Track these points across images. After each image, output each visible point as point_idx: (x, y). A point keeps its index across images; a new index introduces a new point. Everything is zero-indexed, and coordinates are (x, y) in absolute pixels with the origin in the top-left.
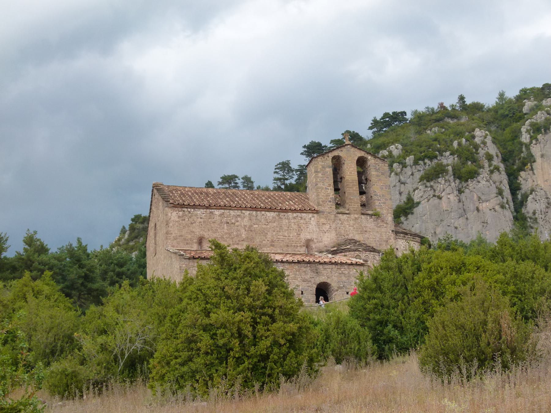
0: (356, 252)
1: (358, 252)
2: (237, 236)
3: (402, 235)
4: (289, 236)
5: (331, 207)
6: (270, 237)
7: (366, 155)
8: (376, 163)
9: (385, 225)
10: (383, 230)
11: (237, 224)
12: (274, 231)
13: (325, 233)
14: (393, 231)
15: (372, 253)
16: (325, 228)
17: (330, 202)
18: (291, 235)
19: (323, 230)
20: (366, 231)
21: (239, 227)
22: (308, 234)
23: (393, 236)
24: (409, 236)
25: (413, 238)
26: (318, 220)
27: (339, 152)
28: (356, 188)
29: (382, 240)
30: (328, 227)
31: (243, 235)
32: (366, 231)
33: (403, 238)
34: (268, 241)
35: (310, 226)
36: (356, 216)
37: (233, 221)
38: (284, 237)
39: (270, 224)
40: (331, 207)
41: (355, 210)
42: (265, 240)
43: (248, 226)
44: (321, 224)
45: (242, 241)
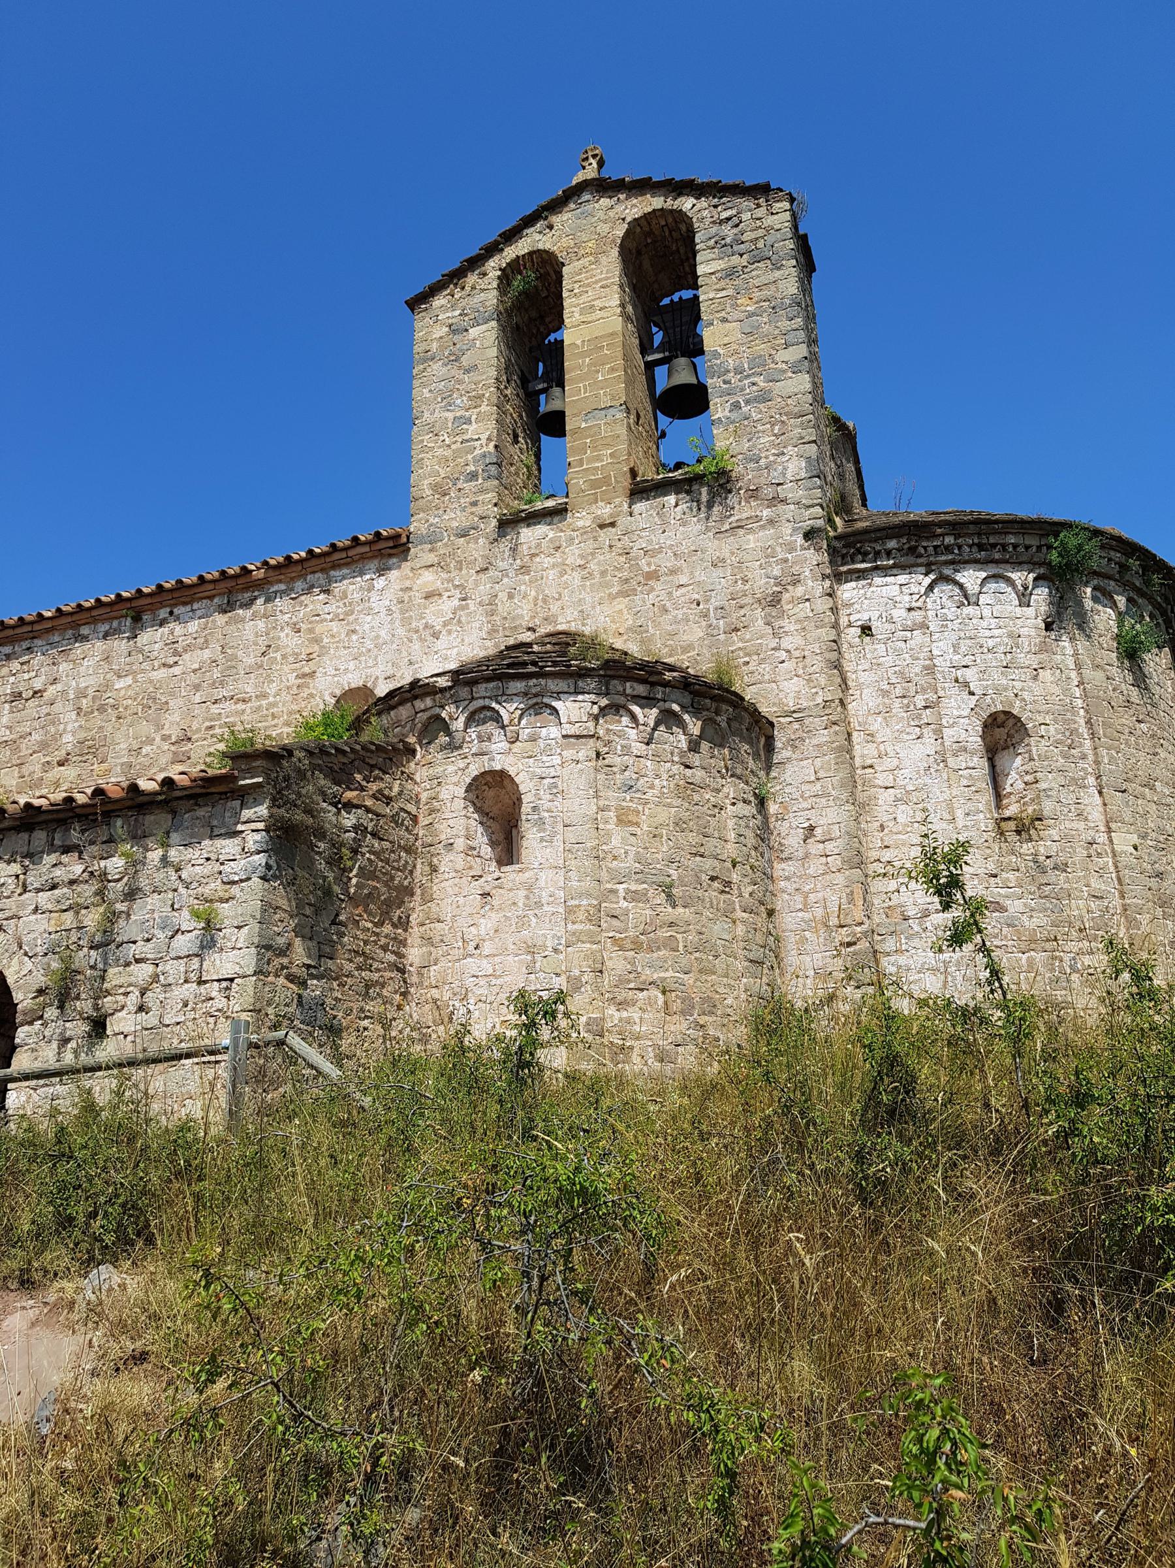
0: (419, 704)
1: (428, 702)
2: (43, 746)
3: (892, 544)
4: (264, 696)
5: (474, 504)
6: (176, 717)
7: (671, 204)
8: (725, 215)
9: (766, 513)
10: (752, 541)
11: (51, 691)
12: (197, 687)
13: (436, 635)
14: (809, 535)
15: (518, 686)
16: (440, 613)
17: (473, 476)
18: (272, 689)
19: (426, 626)
20: (653, 576)
21: (58, 707)
22: (352, 665)
23: (812, 559)
24: (949, 540)
25: (981, 547)
26: (408, 584)
27: (538, 237)
28: (613, 370)
29: (748, 600)
30: (448, 605)
31: (68, 738)
32: (653, 576)
33: (911, 559)
34: (165, 738)
35: (367, 623)
36: (604, 511)
37: (38, 684)
38: (240, 706)
39: (186, 657)
40: (474, 504)
41: (595, 484)
42: (150, 741)
43: (90, 691)
44: (418, 600)
45: (61, 764)
